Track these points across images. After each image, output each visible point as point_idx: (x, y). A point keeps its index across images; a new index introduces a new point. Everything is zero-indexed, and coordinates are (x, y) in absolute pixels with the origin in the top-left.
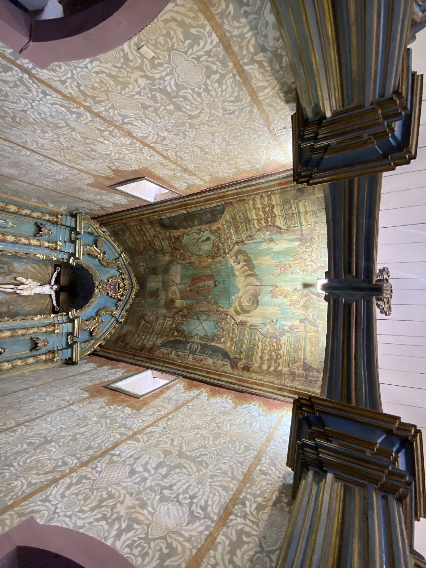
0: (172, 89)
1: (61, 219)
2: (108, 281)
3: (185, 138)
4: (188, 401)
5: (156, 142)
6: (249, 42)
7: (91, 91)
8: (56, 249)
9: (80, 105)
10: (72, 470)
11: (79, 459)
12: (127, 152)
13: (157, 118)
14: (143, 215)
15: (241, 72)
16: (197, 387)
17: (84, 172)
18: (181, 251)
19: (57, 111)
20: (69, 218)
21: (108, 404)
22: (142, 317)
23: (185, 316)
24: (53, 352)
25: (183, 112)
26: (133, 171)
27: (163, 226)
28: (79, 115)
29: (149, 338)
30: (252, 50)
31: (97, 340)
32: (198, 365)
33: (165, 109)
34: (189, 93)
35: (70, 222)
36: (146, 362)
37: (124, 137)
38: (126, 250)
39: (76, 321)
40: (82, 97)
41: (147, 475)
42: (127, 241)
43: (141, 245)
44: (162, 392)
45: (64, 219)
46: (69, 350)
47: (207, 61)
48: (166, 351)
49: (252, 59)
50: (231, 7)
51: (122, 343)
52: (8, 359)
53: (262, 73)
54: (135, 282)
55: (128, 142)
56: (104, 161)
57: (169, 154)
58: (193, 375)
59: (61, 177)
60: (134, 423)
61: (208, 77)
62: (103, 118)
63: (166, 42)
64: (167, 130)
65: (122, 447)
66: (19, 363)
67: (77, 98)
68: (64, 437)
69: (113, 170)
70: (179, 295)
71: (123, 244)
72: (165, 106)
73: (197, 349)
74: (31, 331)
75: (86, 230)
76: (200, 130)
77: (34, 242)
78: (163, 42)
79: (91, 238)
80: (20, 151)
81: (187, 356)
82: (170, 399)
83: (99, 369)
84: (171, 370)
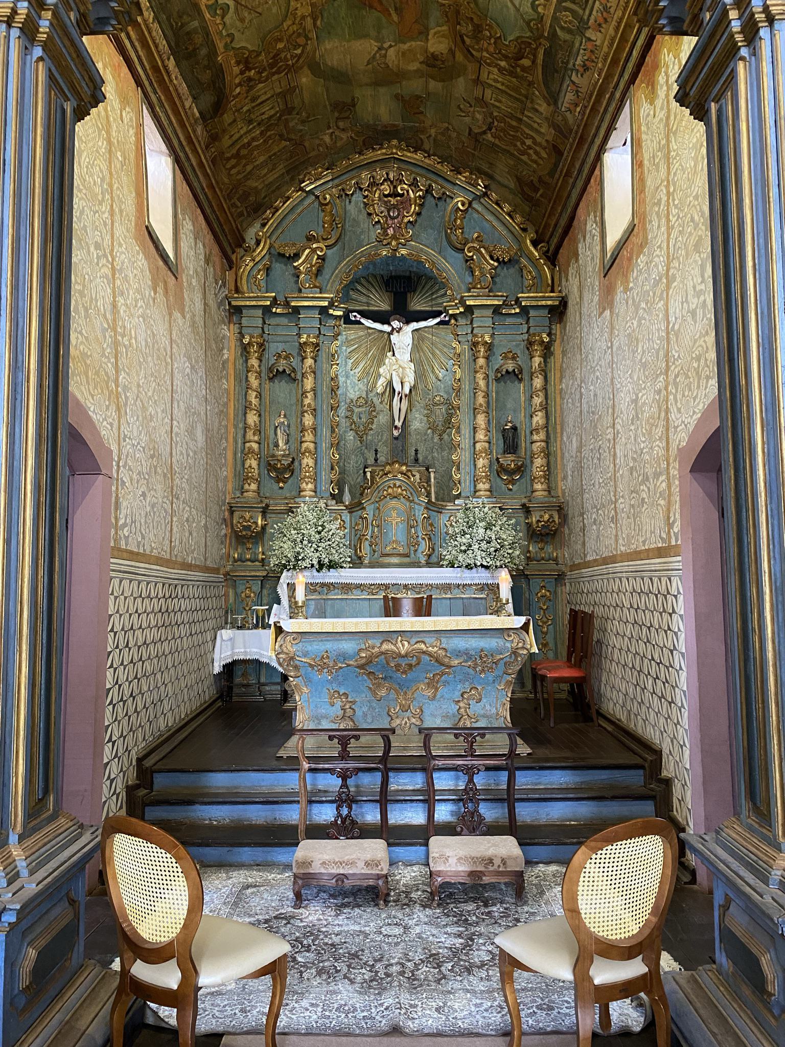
1: (252, 337)
2: (379, 221)
3: (83, 208)
4: (668, 118)
5: (105, 256)
8: (317, 345)
9: (118, 395)
10: (666, 388)
11: (661, 373)
12: (131, 292)
14: (201, 164)
16: (656, 66)
18: (280, 45)
19: (132, 416)
20: (244, 322)
21: (627, 289)
22: (475, 138)
23: (478, 29)
24: (530, 343)
26: (146, 259)
27: (218, 107)
28: (125, 389)
29: (532, 129)
31: (520, 249)
32: (611, 31)
35: (253, 320)
36: (587, 154)
37: (119, 312)
38: (292, 179)
39: (468, 303)
41: (702, 298)
42: (271, 179)
43: (276, 149)
44: (641, 165)
45: (250, 330)
46: (532, 313)
48: (570, 96)
51: (536, 190)
52: (527, 415)
54: (380, 153)
55: (120, 300)
57: (106, 215)
58: (635, 53)
59: (187, 364)
60: (656, 266)
65: (671, 311)
66: (537, 401)
68: (639, 379)
69: (155, 294)
70: (413, 43)
71: (278, 188)
73: (572, 12)
74: (482, 383)
75: (263, 284)
77: (309, 383)
79: (278, 267)
80: (177, 434)
81: (590, 46)
82: (654, 157)
83: (580, 262)
84: (613, 105)
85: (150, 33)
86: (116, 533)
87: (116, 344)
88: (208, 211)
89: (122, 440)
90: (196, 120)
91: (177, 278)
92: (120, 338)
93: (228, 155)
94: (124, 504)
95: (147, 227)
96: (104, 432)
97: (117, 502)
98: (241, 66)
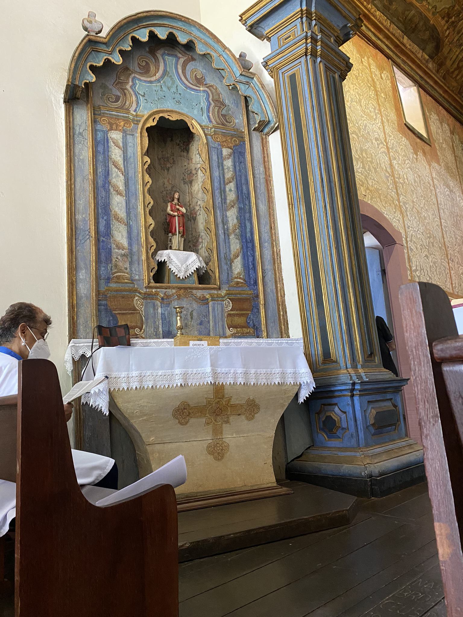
5: (382, 143)
9: (400, 207)
12: (400, 157)
14: (436, 82)
17: (432, 175)
19: (411, 216)
26: (407, 139)
27: (438, 48)
28: (405, 203)
37: (394, 168)
55: (395, 162)
56: (416, 168)
57: (380, 124)
62: (396, 189)
69: (417, 156)
80: (445, 227)
85: (389, 30)
86: (411, 273)
87: (395, 183)
88: (447, 105)
89: (407, 229)
90: (427, 61)
91: (431, 146)
93: (452, 70)
94: (414, 260)
95: (405, 124)
96: (395, 224)
98: (446, 19)
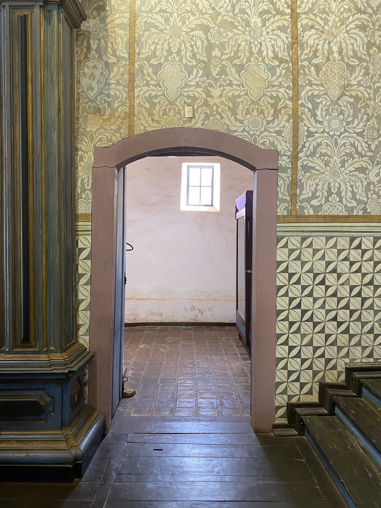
0: (198, 71)
6: (115, 76)
7: (266, 113)
13: (241, 48)
15: (132, 54)
19: (328, 113)
25: (209, 41)
30: (115, 69)
33: (223, 54)
34: (186, 59)
40: (283, 111)
47: (152, 79)
49: (118, 61)
50: (116, 106)
53: (116, 43)
61: (160, 65)
62: (295, 81)
63: (170, 110)
64: (248, 24)
67: (288, 114)
72: (220, 58)
76: (210, 5)
78: (172, 111)
92: (305, 63)
97: (294, 184)
